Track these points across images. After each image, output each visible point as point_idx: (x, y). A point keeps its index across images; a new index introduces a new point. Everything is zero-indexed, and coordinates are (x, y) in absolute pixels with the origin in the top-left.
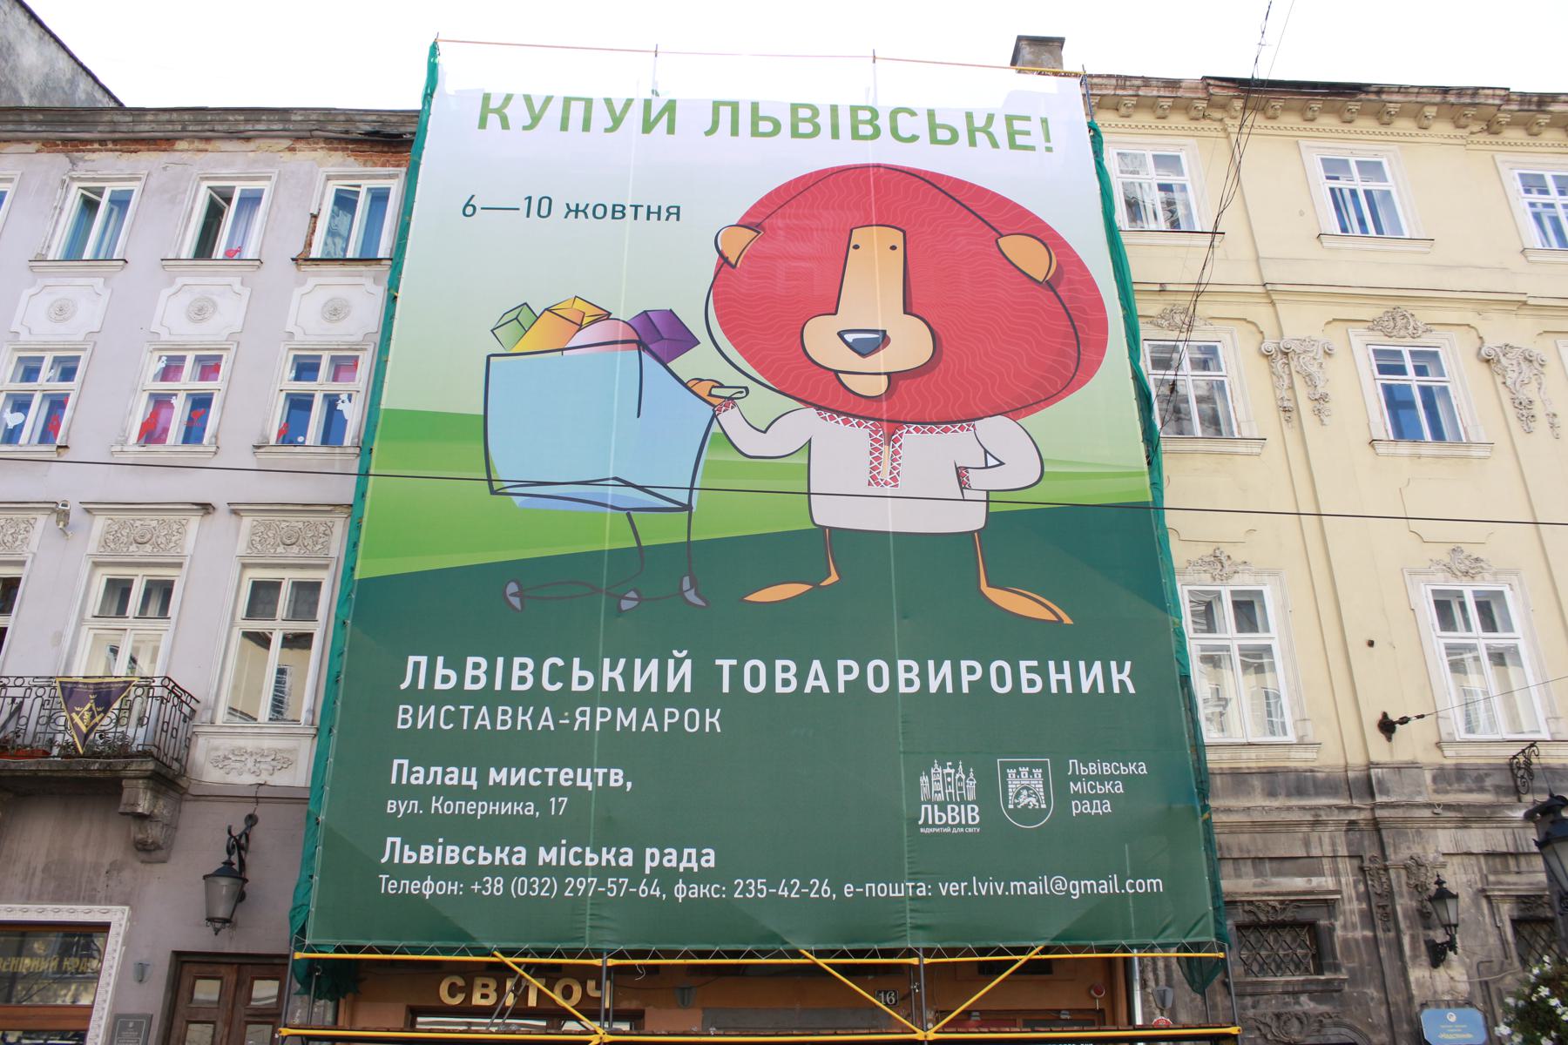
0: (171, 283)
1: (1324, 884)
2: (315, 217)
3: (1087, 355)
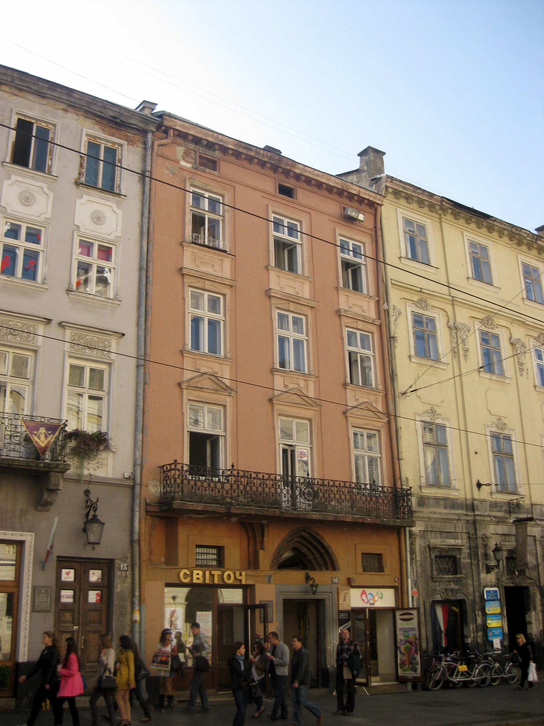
0: (9, 178)
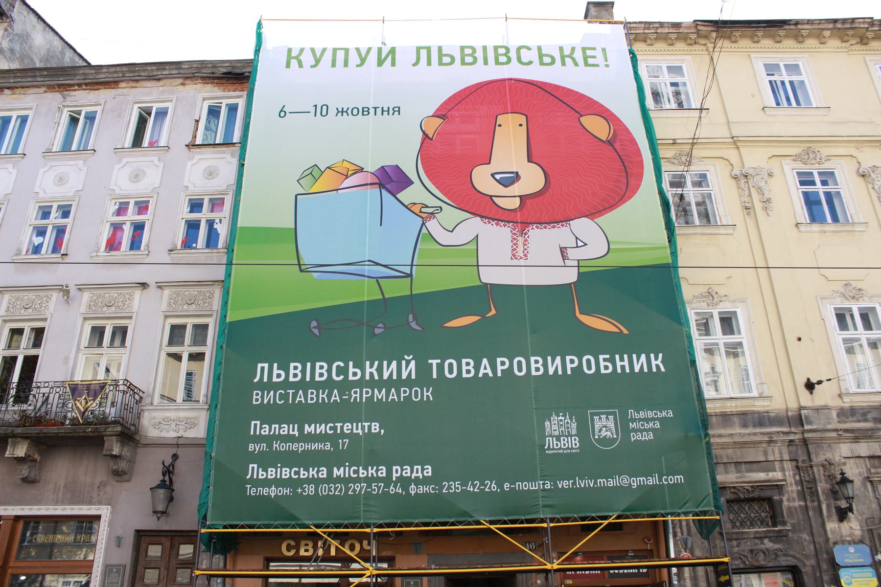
0: (120, 162)
1: (776, 476)
2: (197, 121)
3: (632, 182)
